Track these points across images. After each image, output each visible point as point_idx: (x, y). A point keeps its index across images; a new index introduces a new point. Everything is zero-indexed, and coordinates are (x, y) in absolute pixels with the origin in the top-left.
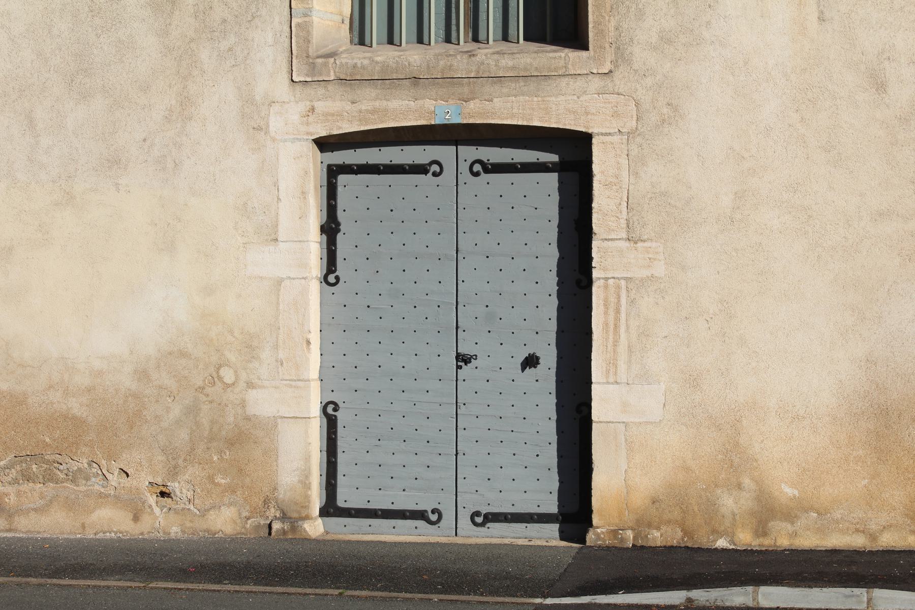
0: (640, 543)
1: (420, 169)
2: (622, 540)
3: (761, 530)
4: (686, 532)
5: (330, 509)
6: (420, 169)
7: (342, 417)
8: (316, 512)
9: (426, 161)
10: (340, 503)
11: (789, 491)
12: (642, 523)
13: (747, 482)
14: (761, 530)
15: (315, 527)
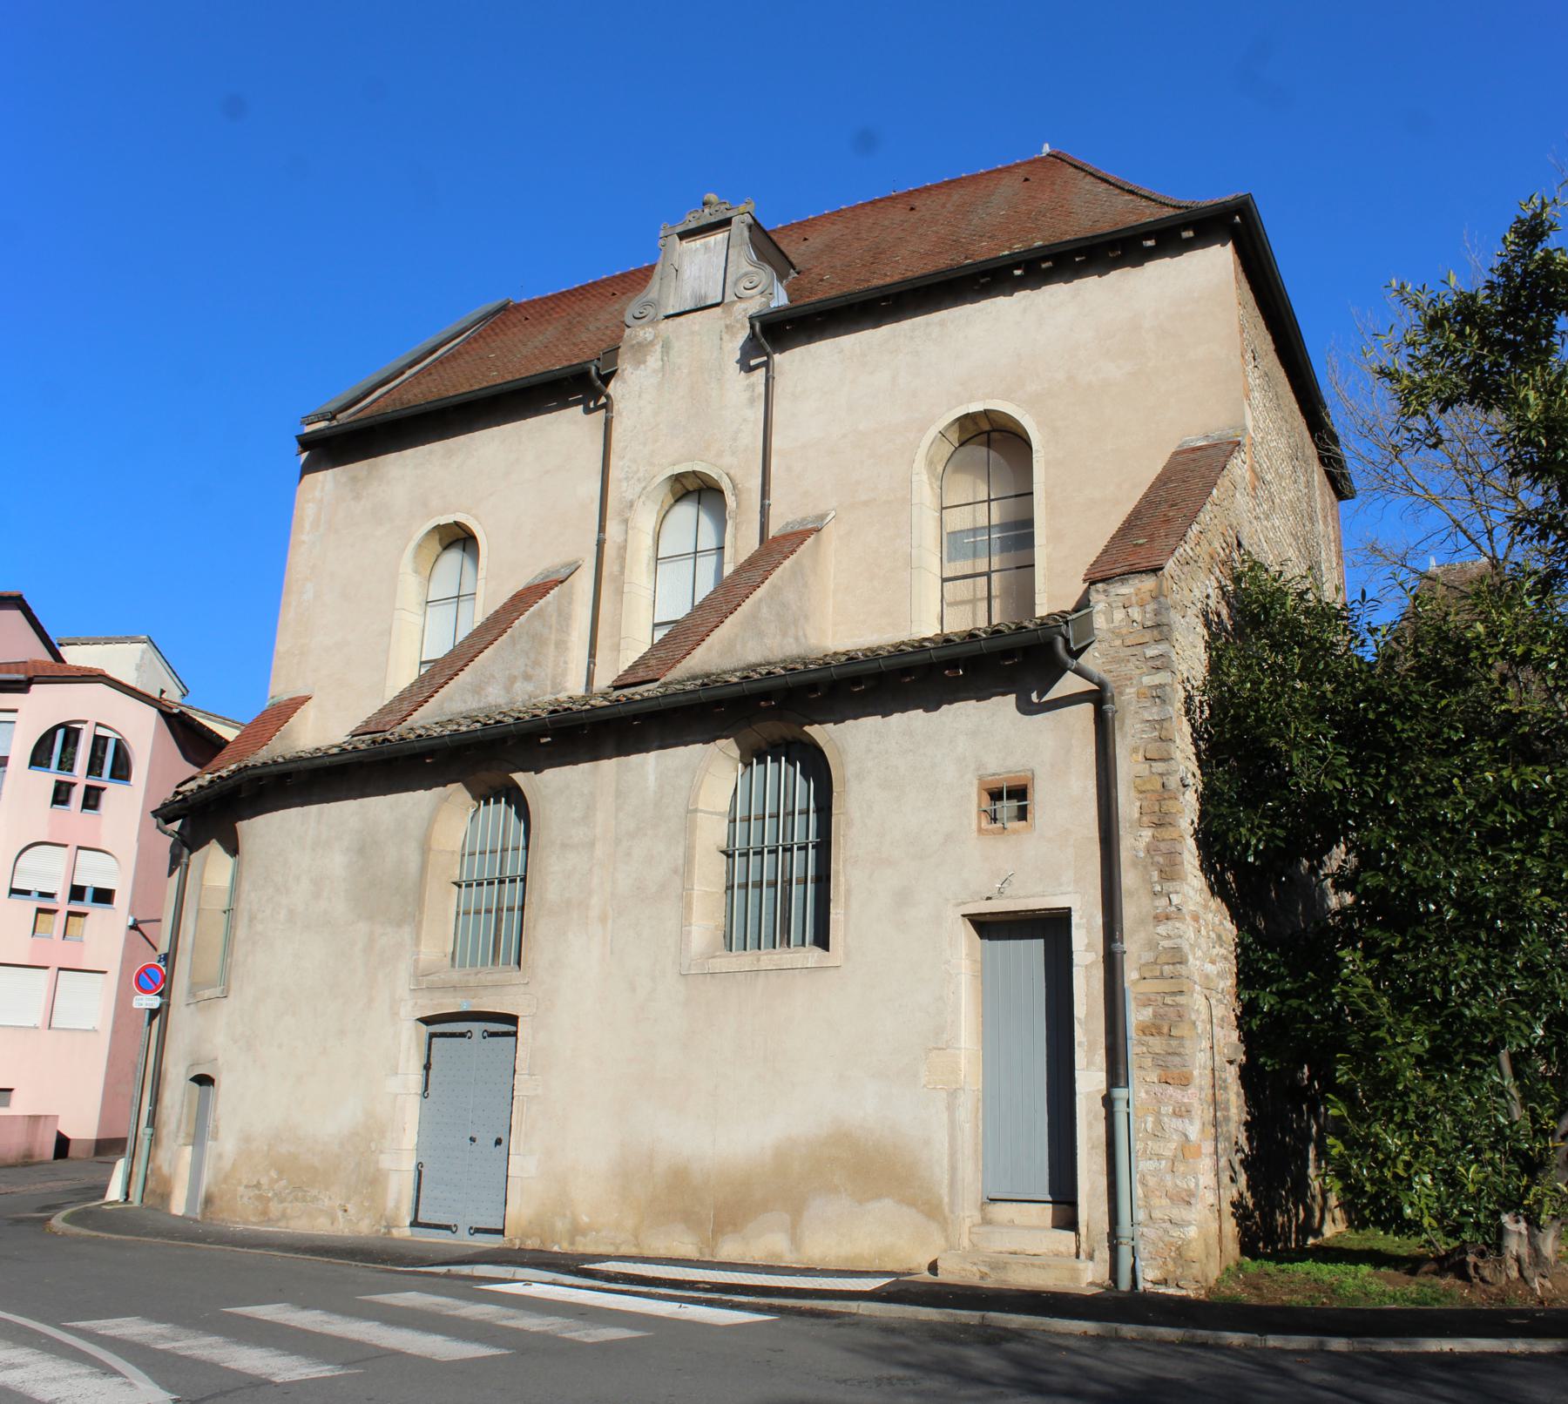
0: (523, 1247)
1: (462, 1035)
2: (514, 1245)
3: (572, 1243)
4: (542, 1242)
5: (415, 1223)
6: (462, 1035)
7: (424, 1170)
8: (408, 1223)
9: (465, 1030)
10: (420, 1220)
11: (585, 1219)
12: (526, 1235)
13: (568, 1213)
14: (572, 1243)
15: (404, 1231)
